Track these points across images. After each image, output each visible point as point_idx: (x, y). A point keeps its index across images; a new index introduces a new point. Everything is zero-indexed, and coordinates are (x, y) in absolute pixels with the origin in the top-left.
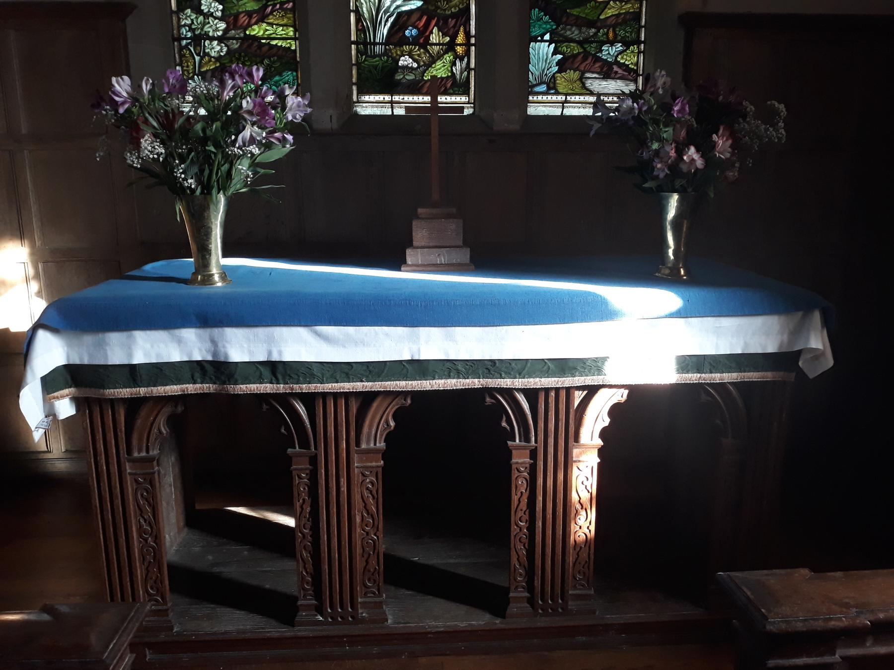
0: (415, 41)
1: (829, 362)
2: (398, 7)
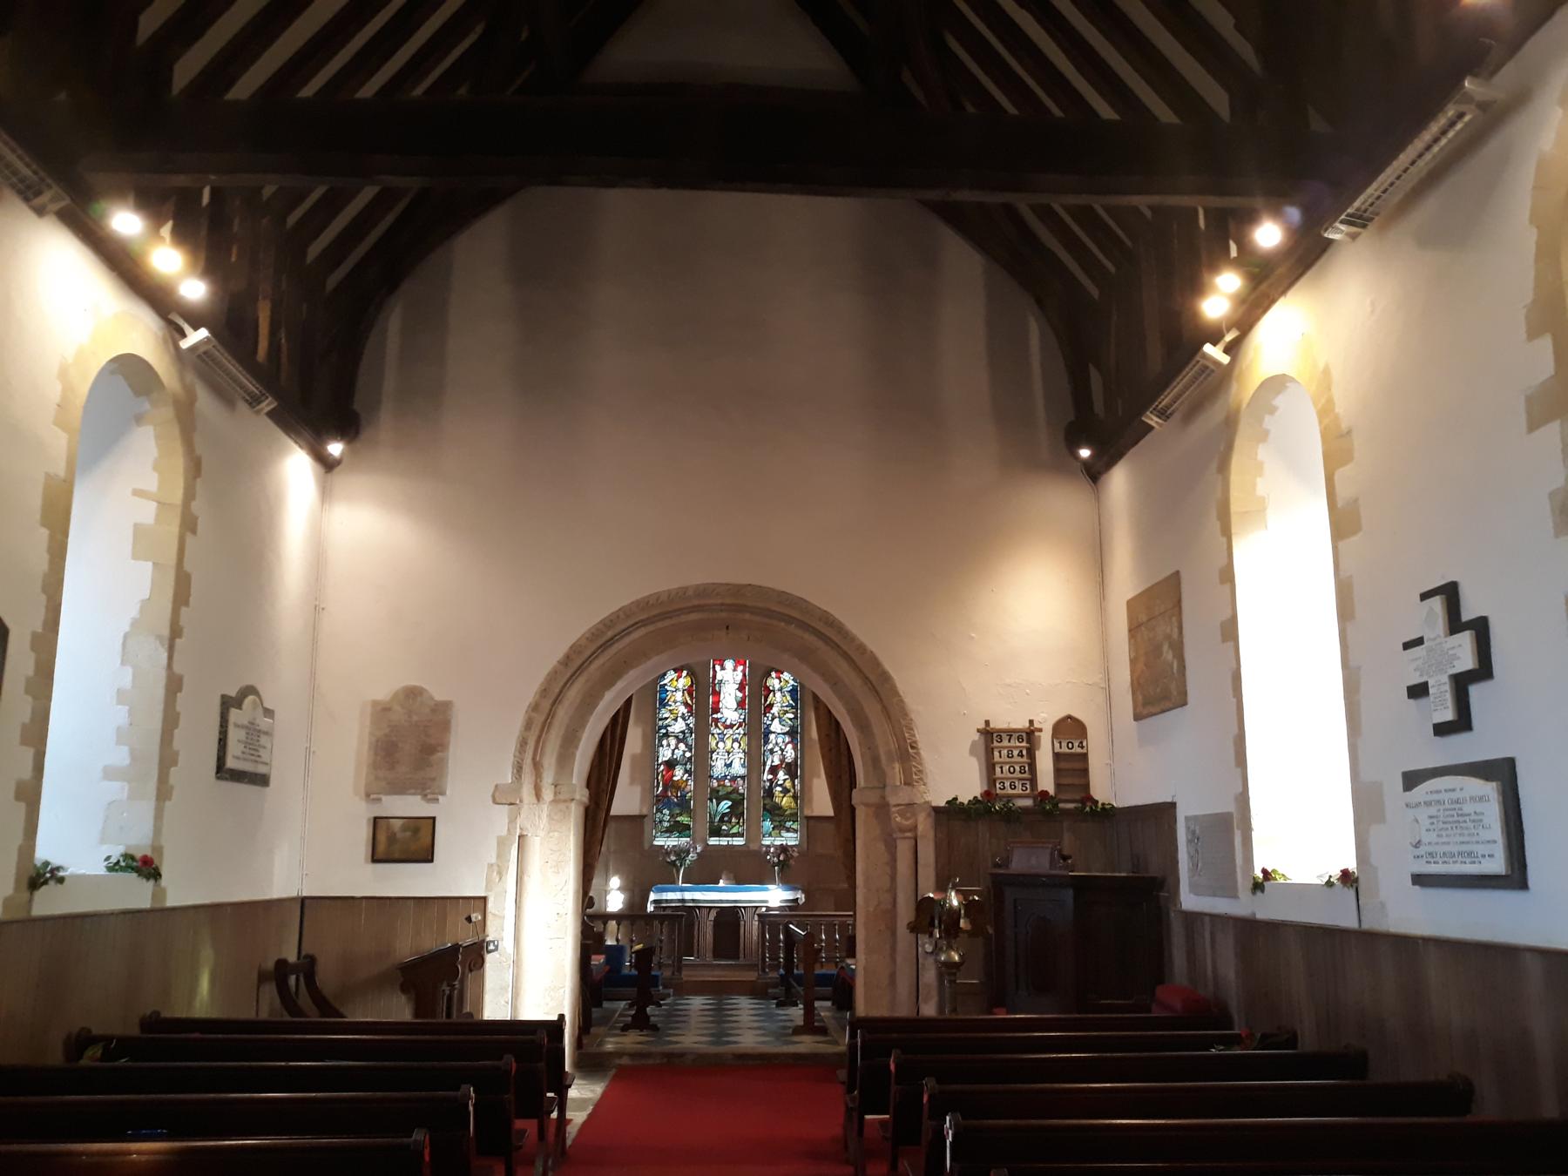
0: (727, 821)
1: (804, 900)
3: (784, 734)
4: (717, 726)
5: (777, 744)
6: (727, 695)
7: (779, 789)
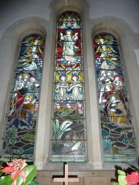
2: (64, 130)
3: (111, 70)
4: (60, 66)
5: (107, 77)
6: (68, 48)
7: (113, 110)
